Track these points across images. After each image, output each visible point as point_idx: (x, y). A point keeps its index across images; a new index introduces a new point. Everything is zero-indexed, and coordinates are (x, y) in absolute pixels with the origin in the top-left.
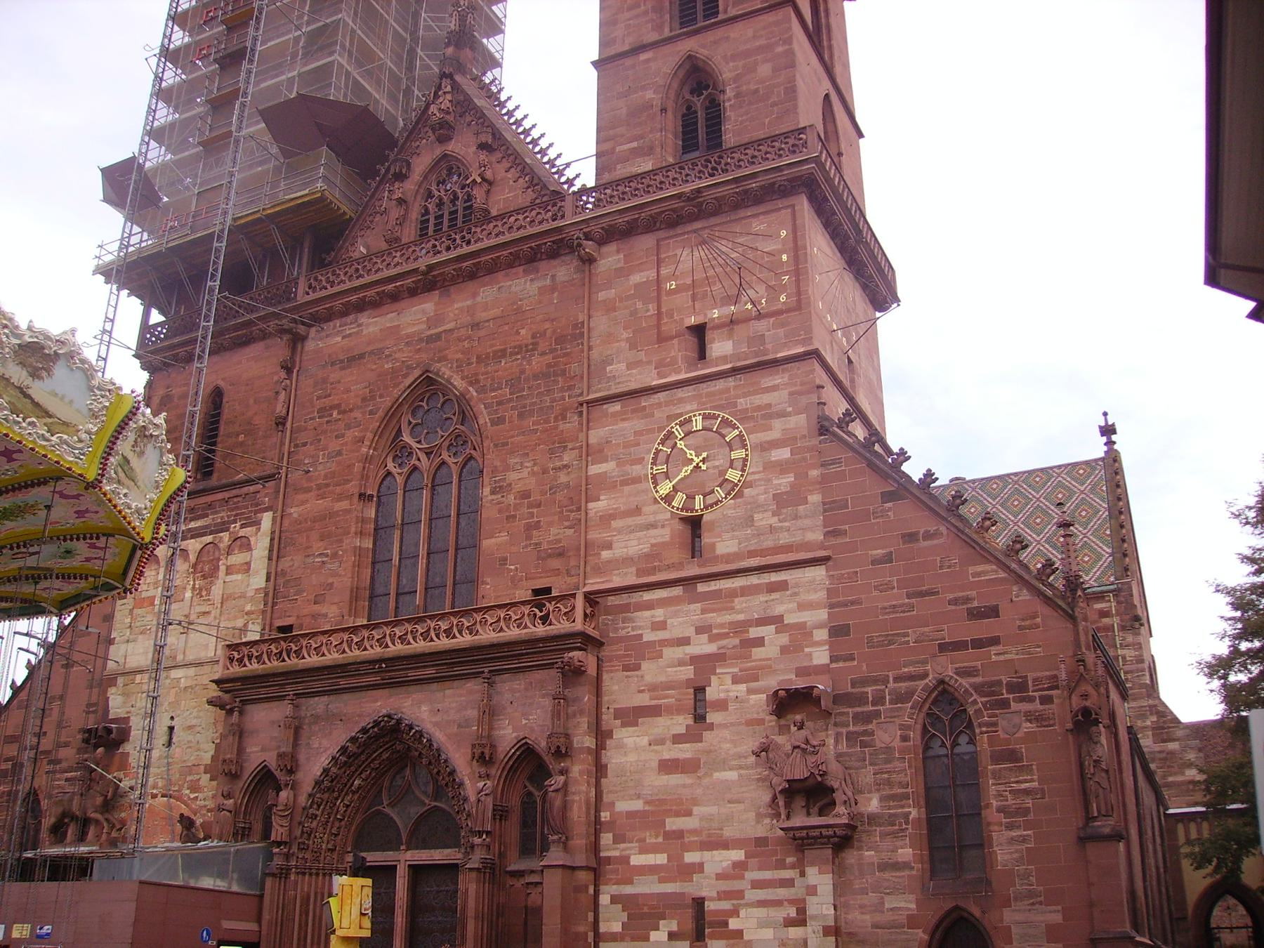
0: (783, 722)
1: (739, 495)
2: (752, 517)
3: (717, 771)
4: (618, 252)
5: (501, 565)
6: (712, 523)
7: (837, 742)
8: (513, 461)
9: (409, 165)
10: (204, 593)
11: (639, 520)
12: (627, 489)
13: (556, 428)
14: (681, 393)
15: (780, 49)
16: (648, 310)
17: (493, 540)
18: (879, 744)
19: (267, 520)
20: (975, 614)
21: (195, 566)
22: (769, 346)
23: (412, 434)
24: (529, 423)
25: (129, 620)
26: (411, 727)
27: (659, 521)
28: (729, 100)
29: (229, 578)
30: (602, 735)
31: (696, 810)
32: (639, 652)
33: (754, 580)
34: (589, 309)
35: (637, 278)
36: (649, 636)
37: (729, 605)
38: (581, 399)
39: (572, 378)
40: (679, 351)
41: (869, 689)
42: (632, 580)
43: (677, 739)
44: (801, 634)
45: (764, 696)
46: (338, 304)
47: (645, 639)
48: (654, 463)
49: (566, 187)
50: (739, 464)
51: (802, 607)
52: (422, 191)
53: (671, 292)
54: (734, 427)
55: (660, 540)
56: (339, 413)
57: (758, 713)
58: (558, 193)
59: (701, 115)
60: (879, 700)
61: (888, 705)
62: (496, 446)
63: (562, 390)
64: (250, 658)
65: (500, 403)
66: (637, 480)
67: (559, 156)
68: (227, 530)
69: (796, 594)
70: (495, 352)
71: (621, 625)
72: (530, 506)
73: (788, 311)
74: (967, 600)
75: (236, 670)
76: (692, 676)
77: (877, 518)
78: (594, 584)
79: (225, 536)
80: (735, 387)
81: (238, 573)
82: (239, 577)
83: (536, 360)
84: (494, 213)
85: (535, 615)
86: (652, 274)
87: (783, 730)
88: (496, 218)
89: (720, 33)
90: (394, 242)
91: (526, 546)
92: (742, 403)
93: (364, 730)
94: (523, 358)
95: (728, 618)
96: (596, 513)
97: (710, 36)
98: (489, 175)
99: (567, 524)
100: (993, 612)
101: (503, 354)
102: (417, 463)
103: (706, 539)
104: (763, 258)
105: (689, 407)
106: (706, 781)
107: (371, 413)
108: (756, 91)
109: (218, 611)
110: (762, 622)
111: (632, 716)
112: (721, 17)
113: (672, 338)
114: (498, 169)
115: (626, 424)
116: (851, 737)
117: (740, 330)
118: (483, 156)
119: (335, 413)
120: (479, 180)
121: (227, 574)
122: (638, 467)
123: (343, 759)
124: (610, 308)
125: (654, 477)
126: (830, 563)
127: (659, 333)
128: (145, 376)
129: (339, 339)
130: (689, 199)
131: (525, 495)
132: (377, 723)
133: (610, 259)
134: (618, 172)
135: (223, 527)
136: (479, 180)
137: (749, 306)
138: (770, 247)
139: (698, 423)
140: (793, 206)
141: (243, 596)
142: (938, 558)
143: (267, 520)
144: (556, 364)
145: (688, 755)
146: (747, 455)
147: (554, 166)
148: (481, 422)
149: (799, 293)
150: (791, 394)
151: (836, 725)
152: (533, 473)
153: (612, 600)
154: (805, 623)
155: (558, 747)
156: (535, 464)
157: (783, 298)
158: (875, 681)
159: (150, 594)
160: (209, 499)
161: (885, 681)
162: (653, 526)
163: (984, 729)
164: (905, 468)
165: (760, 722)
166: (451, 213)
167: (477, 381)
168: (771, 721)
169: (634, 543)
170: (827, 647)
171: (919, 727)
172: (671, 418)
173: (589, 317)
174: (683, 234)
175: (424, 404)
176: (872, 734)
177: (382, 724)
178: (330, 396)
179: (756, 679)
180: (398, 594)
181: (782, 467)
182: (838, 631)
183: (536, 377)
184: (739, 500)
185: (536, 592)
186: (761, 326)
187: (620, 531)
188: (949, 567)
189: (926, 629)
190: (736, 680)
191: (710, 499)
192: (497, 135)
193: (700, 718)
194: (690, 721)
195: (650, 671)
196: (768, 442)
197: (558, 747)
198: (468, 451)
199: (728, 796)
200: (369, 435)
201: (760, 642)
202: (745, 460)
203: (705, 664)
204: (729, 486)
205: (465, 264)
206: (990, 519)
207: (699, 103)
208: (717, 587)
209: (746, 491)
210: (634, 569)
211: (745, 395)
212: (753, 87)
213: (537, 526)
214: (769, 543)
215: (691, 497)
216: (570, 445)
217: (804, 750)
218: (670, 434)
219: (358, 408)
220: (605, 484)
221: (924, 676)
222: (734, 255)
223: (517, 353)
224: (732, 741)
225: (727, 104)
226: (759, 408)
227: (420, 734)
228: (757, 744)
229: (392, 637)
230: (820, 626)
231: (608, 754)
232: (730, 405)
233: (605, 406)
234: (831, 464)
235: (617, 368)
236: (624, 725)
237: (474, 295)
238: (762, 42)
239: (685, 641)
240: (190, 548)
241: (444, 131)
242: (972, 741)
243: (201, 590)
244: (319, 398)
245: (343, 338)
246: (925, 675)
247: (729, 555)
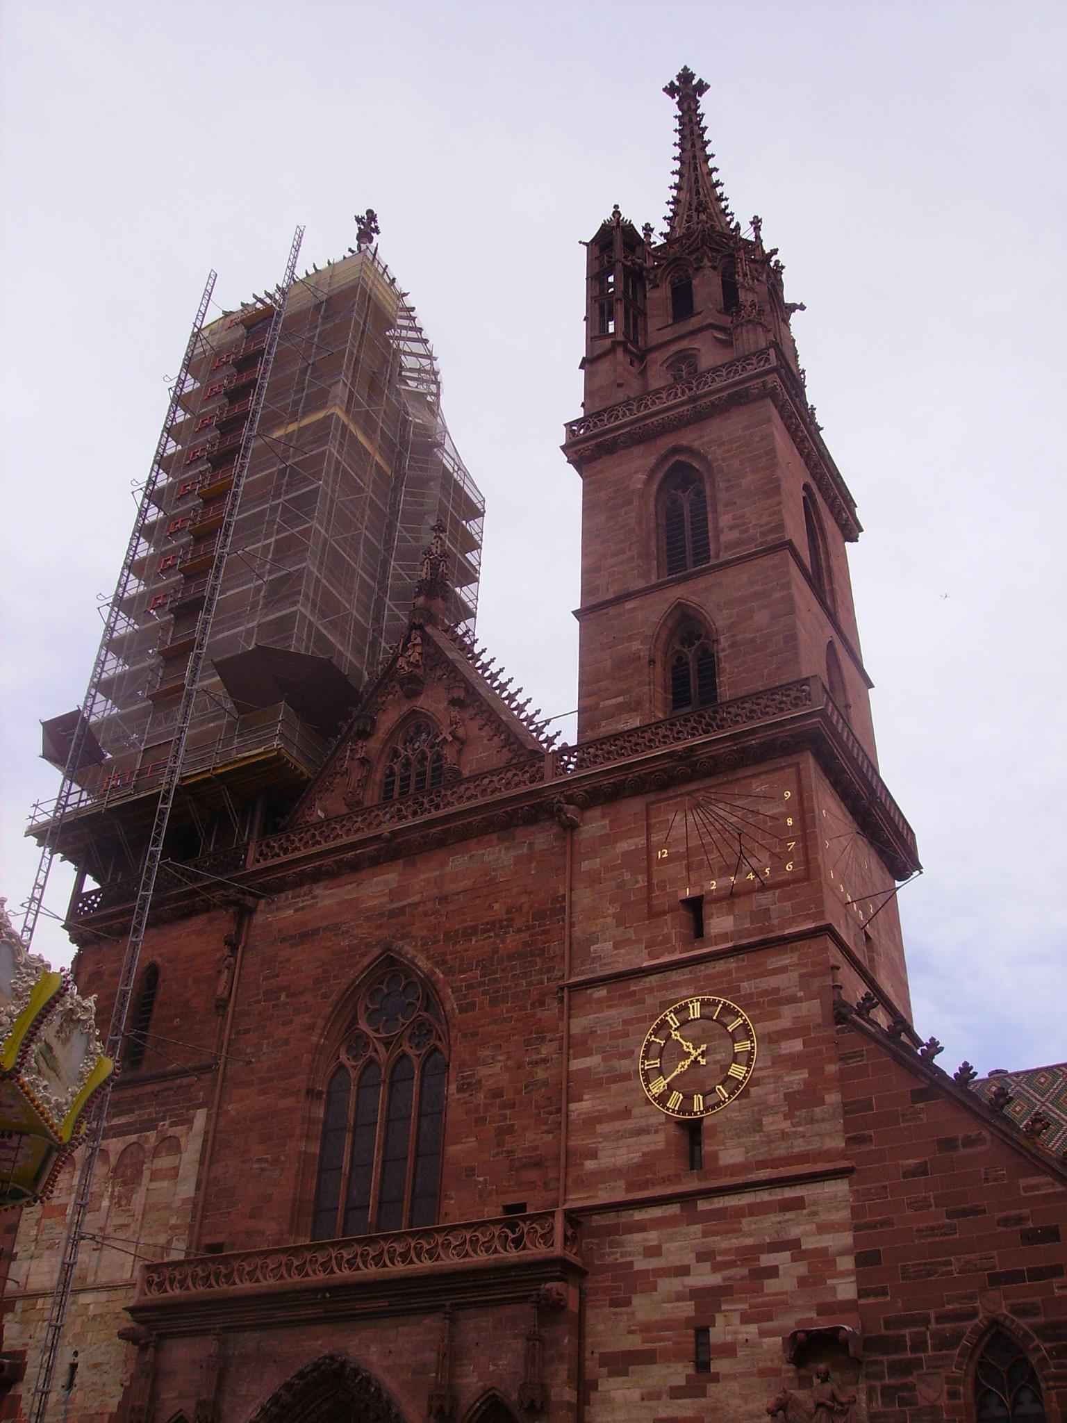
0: (803, 1372)
1: (745, 1093)
2: (761, 1121)
4: (603, 816)
5: (467, 1176)
6: (714, 1127)
7: (870, 1399)
8: (485, 1053)
9: (374, 722)
10: (124, 1202)
11: (629, 1124)
12: (615, 1087)
14: (675, 976)
15: (777, 595)
16: (637, 882)
17: (459, 1147)
18: (922, 1402)
19: (200, 1118)
20: (1030, 1238)
21: (115, 1170)
22: (775, 922)
23: (370, 1021)
25: (35, 1232)
26: (356, 1371)
27: (652, 1125)
28: (723, 650)
29: (153, 1186)
30: (585, 1387)
33: (764, 1196)
34: (571, 882)
35: (624, 846)
36: (640, 1264)
37: (737, 1226)
38: (561, 982)
39: (551, 959)
40: (673, 927)
41: (906, 1332)
42: (620, 1195)
43: (676, 1393)
44: (821, 1262)
45: (779, 1340)
46: (291, 873)
47: (637, 1267)
48: (645, 1058)
49: (545, 745)
50: (744, 1058)
51: (822, 1229)
52: (387, 750)
53: (665, 861)
54: (737, 1015)
55: (653, 1147)
56: (287, 996)
57: (772, 1361)
58: (536, 752)
59: (693, 667)
60: (919, 1345)
61: (930, 1352)
62: (465, 1036)
63: (540, 972)
64: (172, 1282)
65: (470, 987)
66: (626, 1077)
67: (538, 712)
68: (154, 1128)
69: (815, 1213)
71: (608, 1250)
72: (503, 1106)
73: (795, 881)
74: (1019, 1220)
75: (154, 1296)
76: (692, 1314)
77: (908, 1121)
78: (577, 1200)
79: (152, 1136)
80: (738, 968)
81: (164, 1179)
82: (165, 1184)
84: (466, 773)
85: (507, 1237)
86: (642, 841)
87: (804, 1382)
88: (468, 780)
89: (711, 579)
90: (355, 806)
91: (497, 1154)
92: (746, 987)
93: (301, 1375)
94: (497, 935)
95: (735, 1242)
96: (579, 1114)
97: (702, 583)
98: (461, 732)
99: (545, 1128)
100: (1052, 1234)
101: (474, 931)
102: (374, 1054)
103: (707, 1148)
104: (766, 823)
105: (684, 993)
107: (324, 996)
108: (753, 640)
109: (139, 1224)
110: (777, 1247)
111: (621, 1363)
112: (712, 562)
113: (665, 913)
114: (472, 728)
116: (888, 1393)
117: (743, 905)
118: (455, 713)
119: (283, 996)
120: (450, 738)
121: (151, 1180)
122: (626, 1062)
123: (274, 1410)
124: (594, 879)
125: (646, 1073)
126: (854, 1176)
127: (650, 906)
128: (74, 949)
129: (291, 912)
130: (681, 758)
131: (497, 1093)
132: (316, 1366)
133: (594, 825)
134: (603, 730)
135: (150, 1125)
136: (450, 738)
137: (751, 876)
138: (774, 809)
139: (695, 1011)
140: (798, 764)
141: (168, 1206)
142: (983, 1169)
143: (200, 1117)
145: (689, 1413)
146: (753, 1048)
147: (532, 723)
148: (448, 1008)
149: (807, 862)
150: (801, 976)
151: (867, 1376)
152: (507, 1069)
153: (598, 1220)
154: (826, 1249)
155: (533, 1401)
156: (508, 1059)
157: (789, 867)
158: (911, 1321)
159: (60, 1201)
160: (136, 1092)
161: (926, 1321)
163: (1051, 1384)
164: (938, 1060)
165: (775, 1372)
166: (418, 775)
167: (444, 962)
168: (789, 1371)
169: (624, 1150)
170: (853, 1278)
171: (970, 1379)
172: (665, 1005)
173: (571, 890)
174: (676, 797)
175: (384, 987)
176: (912, 1388)
177: (323, 1367)
178: (278, 976)
179: (769, 1317)
180: (347, 1210)
181: (794, 1062)
182: (866, 1259)
183: (511, 957)
184: (744, 1101)
185: (509, 1209)
186: (765, 899)
187: (606, 1137)
188: (996, 1180)
189: (972, 1256)
190: (746, 1319)
191: (711, 1100)
192: (470, 689)
193: (702, 1366)
194: (691, 1370)
195: (643, 1308)
196: (776, 1032)
197: (533, 1401)
198: (432, 1042)
200: (321, 1022)
201: (773, 1272)
202: (751, 1053)
203: (708, 1300)
204: (733, 1084)
205: (433, 830)
206: (1041, 1121)
207: (690, 653)
208: (720, 1205)
209: (753, 1090)
211: (749, 978)
212: (749, 636)
213: (510, 1130)
214: (780, 1151)
215: (688, 1098)
216: (549, 1036)
217: (830, 1409)
218: (664, 1024)
220: (590, 1081)
221: (973, 1314)
222: (733, 819)
223: (489, 931)
225: (722, 655)
226: (765, 993)
227: (368, 1381)
228: (772, 1400)
229: (339, 1260)
230: (843, 1252)
231: (592, 1410)
232: (731, 990)
233: (589, 991)
234: (851, 1058)
235: (603, 947)
236: (611, 1374)
237: (443, 864)
238: (758, 588)
239: (684, 1271)
240: (111, 1148)
241: (413, 686)
242: (1037, 1399)
243: (120, 1198)
244: (266, 978)
246: (973, 1314)
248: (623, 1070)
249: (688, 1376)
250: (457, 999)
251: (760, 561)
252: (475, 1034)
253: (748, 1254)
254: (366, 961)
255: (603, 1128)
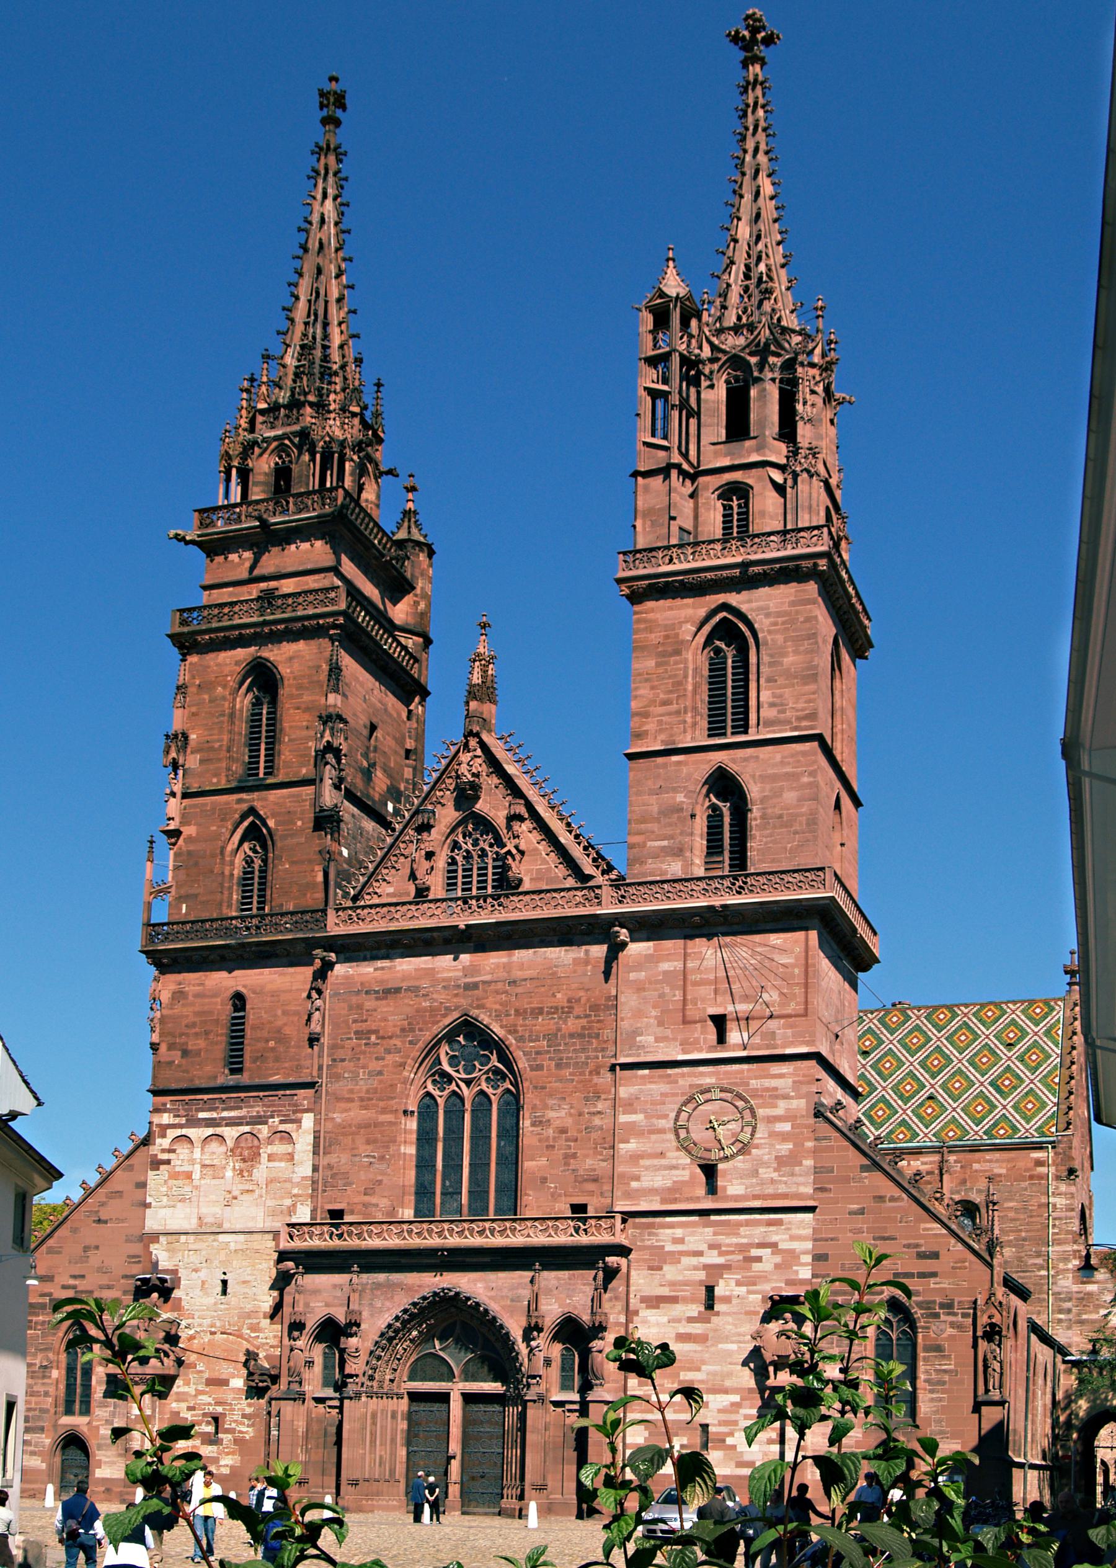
3: (721, 1343)
6: (725, 1171)
8: (551, 1102)
11: (663, 1162)
12: (654, 1137)
13: (590, 1081)
24: (566, 1073)
31: (704, 1368)
32: (658, 1260)
38: (613, 1061)
39: (606, 1042)
43: (690, 1320)
47: (667, 1249)
48: (677, 1119)
55: (680, 1178)
62: (535, 1087)
63: (596, 1050)
65: (537, 1053)
70: (533, 1009)
83: (571, 1022)
94: (560, 1018)
95: (735, 1240)
101: (540, 1011)
106: (713, 1349)
115: (653, 1086)
122: (664, 1121)
144: (590, 1028)
145: (699, 1331)
152: (571, 1115)
162: (674, 1167)
167: (516, 1031)
169: (660, 1178)
183: (572, 1036)
187: (647, 1168)
190: (739, 1283)
193: (710, 1306)
194: (702, 1308)
195: (670, 1272)
199: (729, 1360)
203: (716, 1271)
210: (658, 1198)
216: (603, 1097)
219: (397, 1036)
223: (554, 1013)
224: (733, 1324)
235: (647, 1039)
239: (699, 1254)
245: (376, 969)
247: (737, 1196)
248: (660, 1126)
249: (699, 1312)
250: (528, 1060)
251: (794, 745)
252: (545, 1088)
253: (743, 1248)
254: (447, 1021)
255: (642, 1162)
